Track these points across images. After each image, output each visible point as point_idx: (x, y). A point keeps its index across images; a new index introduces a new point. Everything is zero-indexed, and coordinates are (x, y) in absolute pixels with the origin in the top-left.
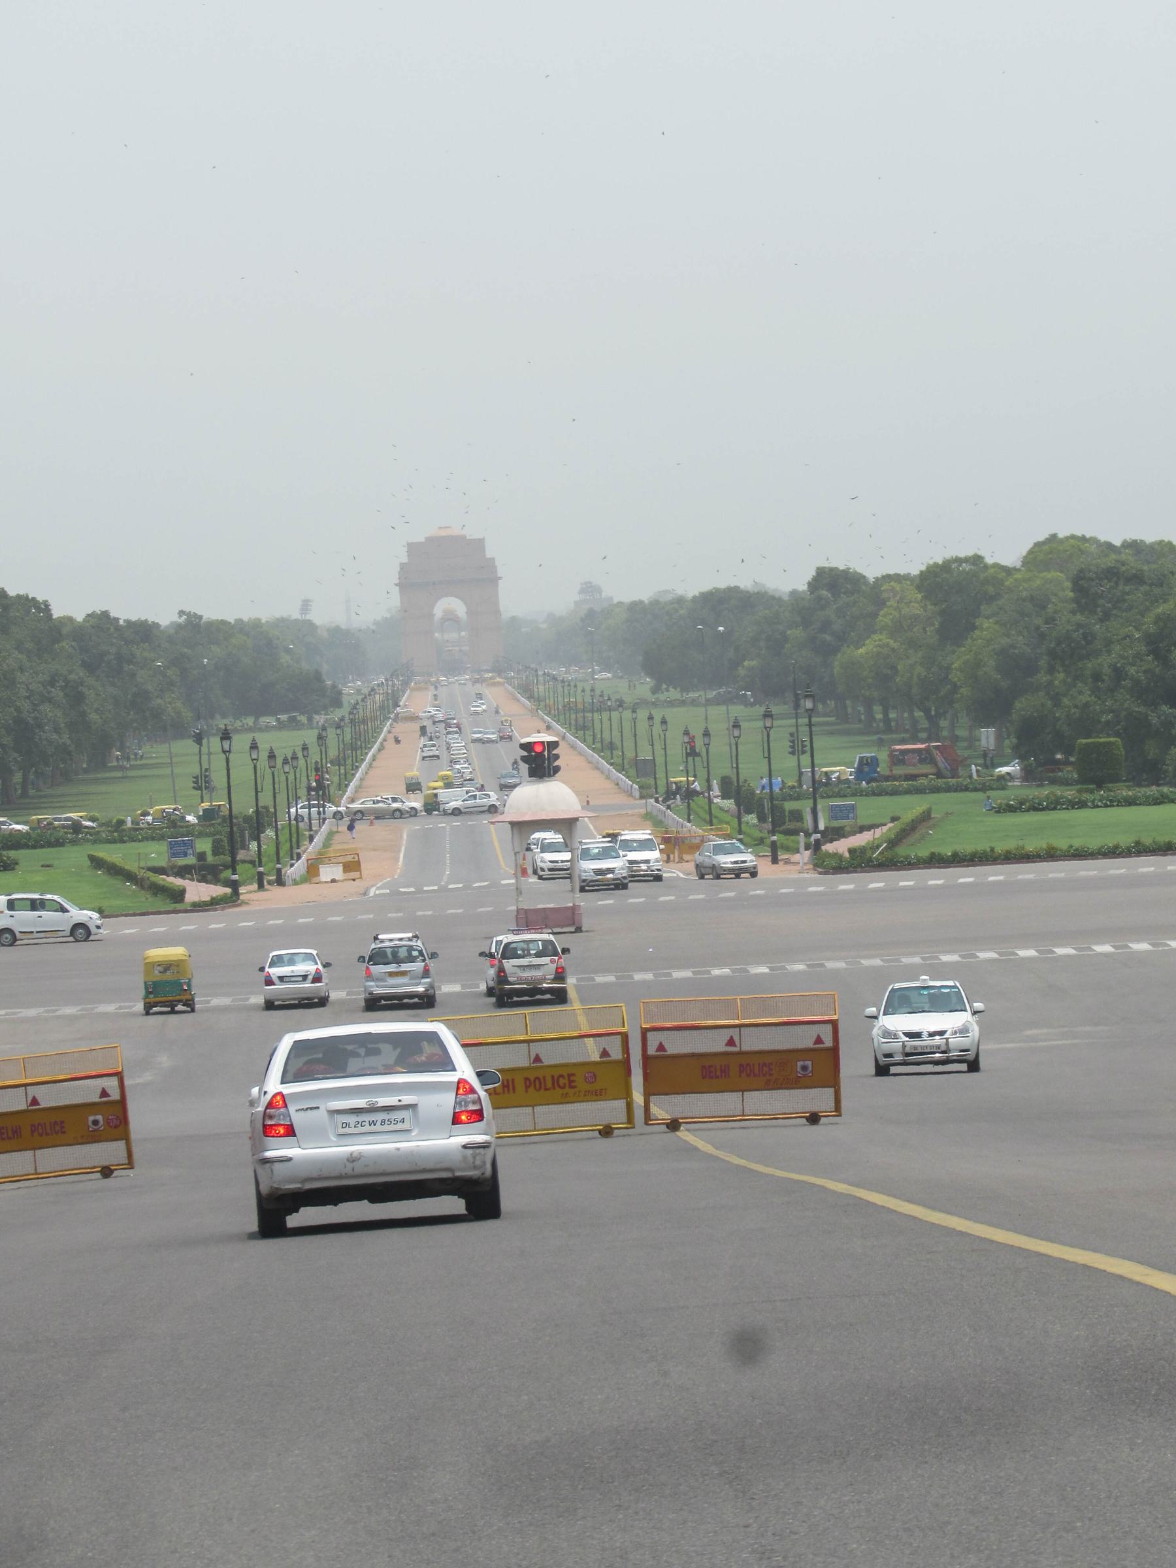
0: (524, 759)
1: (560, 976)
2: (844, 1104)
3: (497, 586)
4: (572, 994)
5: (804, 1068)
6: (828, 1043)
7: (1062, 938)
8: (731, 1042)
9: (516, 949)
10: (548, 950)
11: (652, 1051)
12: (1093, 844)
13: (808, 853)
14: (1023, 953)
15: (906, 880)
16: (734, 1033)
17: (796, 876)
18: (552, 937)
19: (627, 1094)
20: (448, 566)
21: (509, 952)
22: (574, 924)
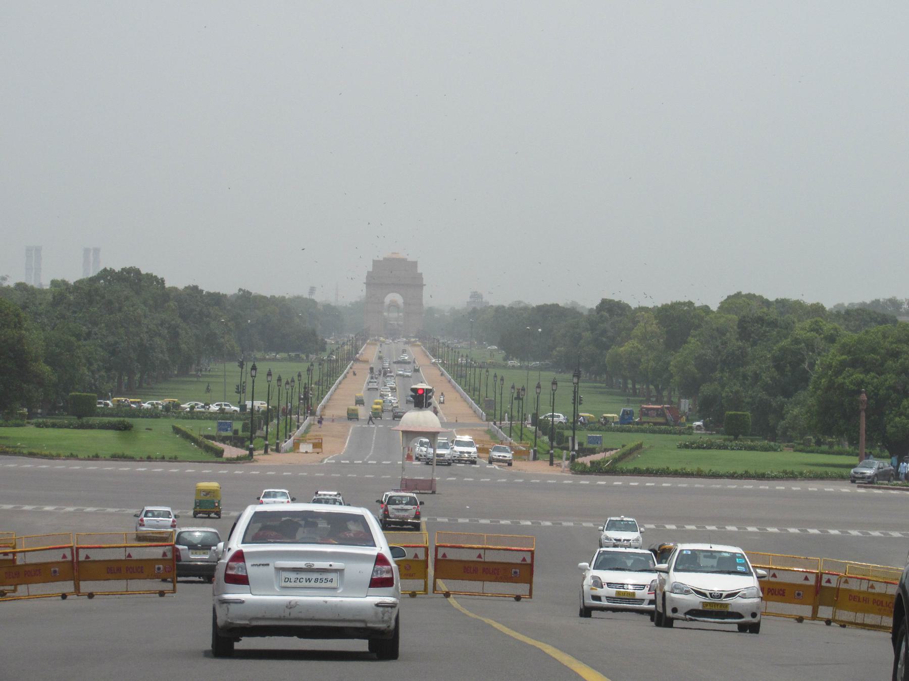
0: (412, 396)
1: (417, 516)
2: (534, 592)
3: (422, 289)
4: (423, 526)
5: (516, 573)
6: (529, 561)
7: (690, 521)
8: (480, 556)
11: (440, 557)
13: (567, 462)
14: (668, 527)
15: (618, 481)
16: (482, 552)
17: (559, 474)
19: (425, 576)
20: (395, 275)
21: (391, 501)
22: (431, 489)
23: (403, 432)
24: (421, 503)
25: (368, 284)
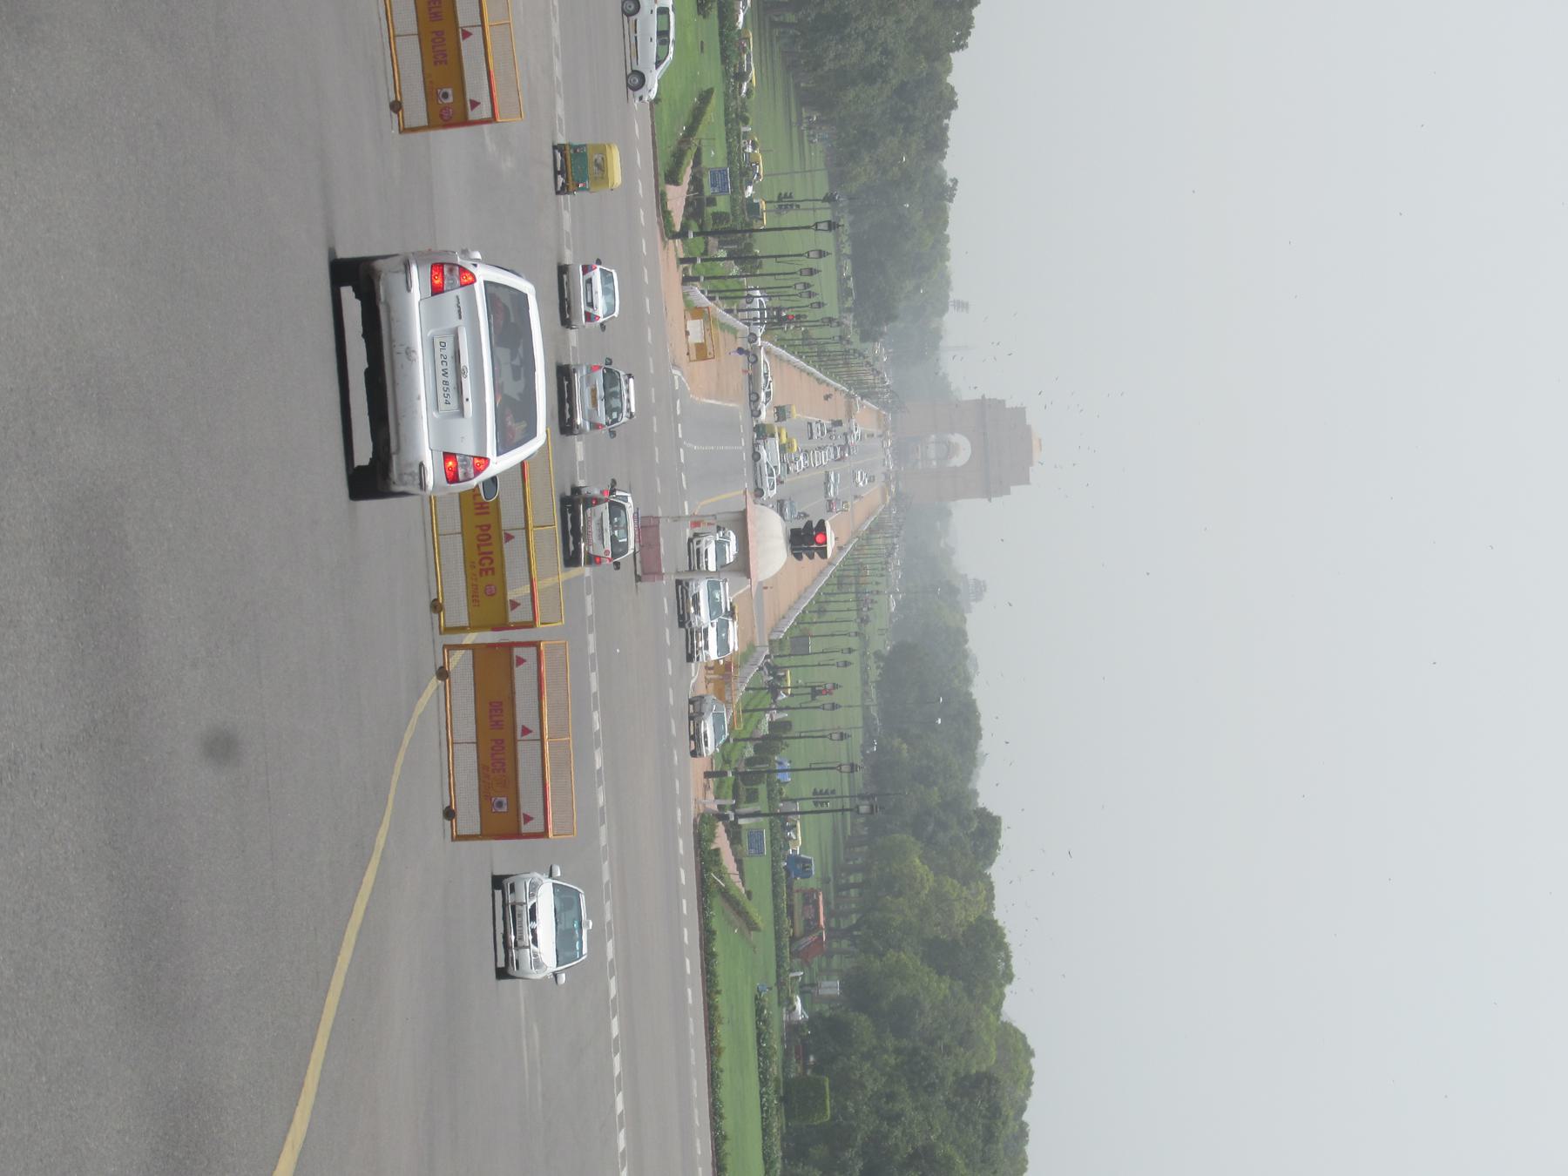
0: (809, 524)
1: (592, 560)
2: (464, 844)
4: (574, 572)
5: (500, 804)
6: (525, 828)
7: (630, 1063)
8: (526, 731)
9: (619, 515)
10: (618, 548)
11: (517, 652)
12: (724, 1093)
14: (615, 1022)
15: (688, 906)
17: (692, 797)
18: (631, 552)
19: (473, 627)
20: (1002, 448)
21: (616, 509)
23: (744, 513)
24: (617, 565)
25: (983, 405)
